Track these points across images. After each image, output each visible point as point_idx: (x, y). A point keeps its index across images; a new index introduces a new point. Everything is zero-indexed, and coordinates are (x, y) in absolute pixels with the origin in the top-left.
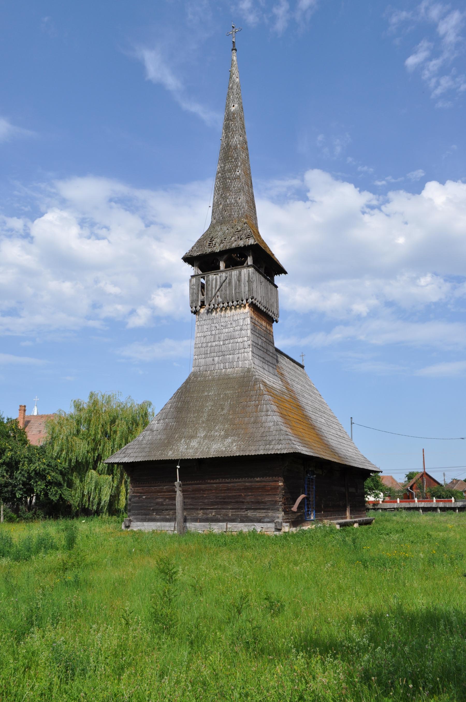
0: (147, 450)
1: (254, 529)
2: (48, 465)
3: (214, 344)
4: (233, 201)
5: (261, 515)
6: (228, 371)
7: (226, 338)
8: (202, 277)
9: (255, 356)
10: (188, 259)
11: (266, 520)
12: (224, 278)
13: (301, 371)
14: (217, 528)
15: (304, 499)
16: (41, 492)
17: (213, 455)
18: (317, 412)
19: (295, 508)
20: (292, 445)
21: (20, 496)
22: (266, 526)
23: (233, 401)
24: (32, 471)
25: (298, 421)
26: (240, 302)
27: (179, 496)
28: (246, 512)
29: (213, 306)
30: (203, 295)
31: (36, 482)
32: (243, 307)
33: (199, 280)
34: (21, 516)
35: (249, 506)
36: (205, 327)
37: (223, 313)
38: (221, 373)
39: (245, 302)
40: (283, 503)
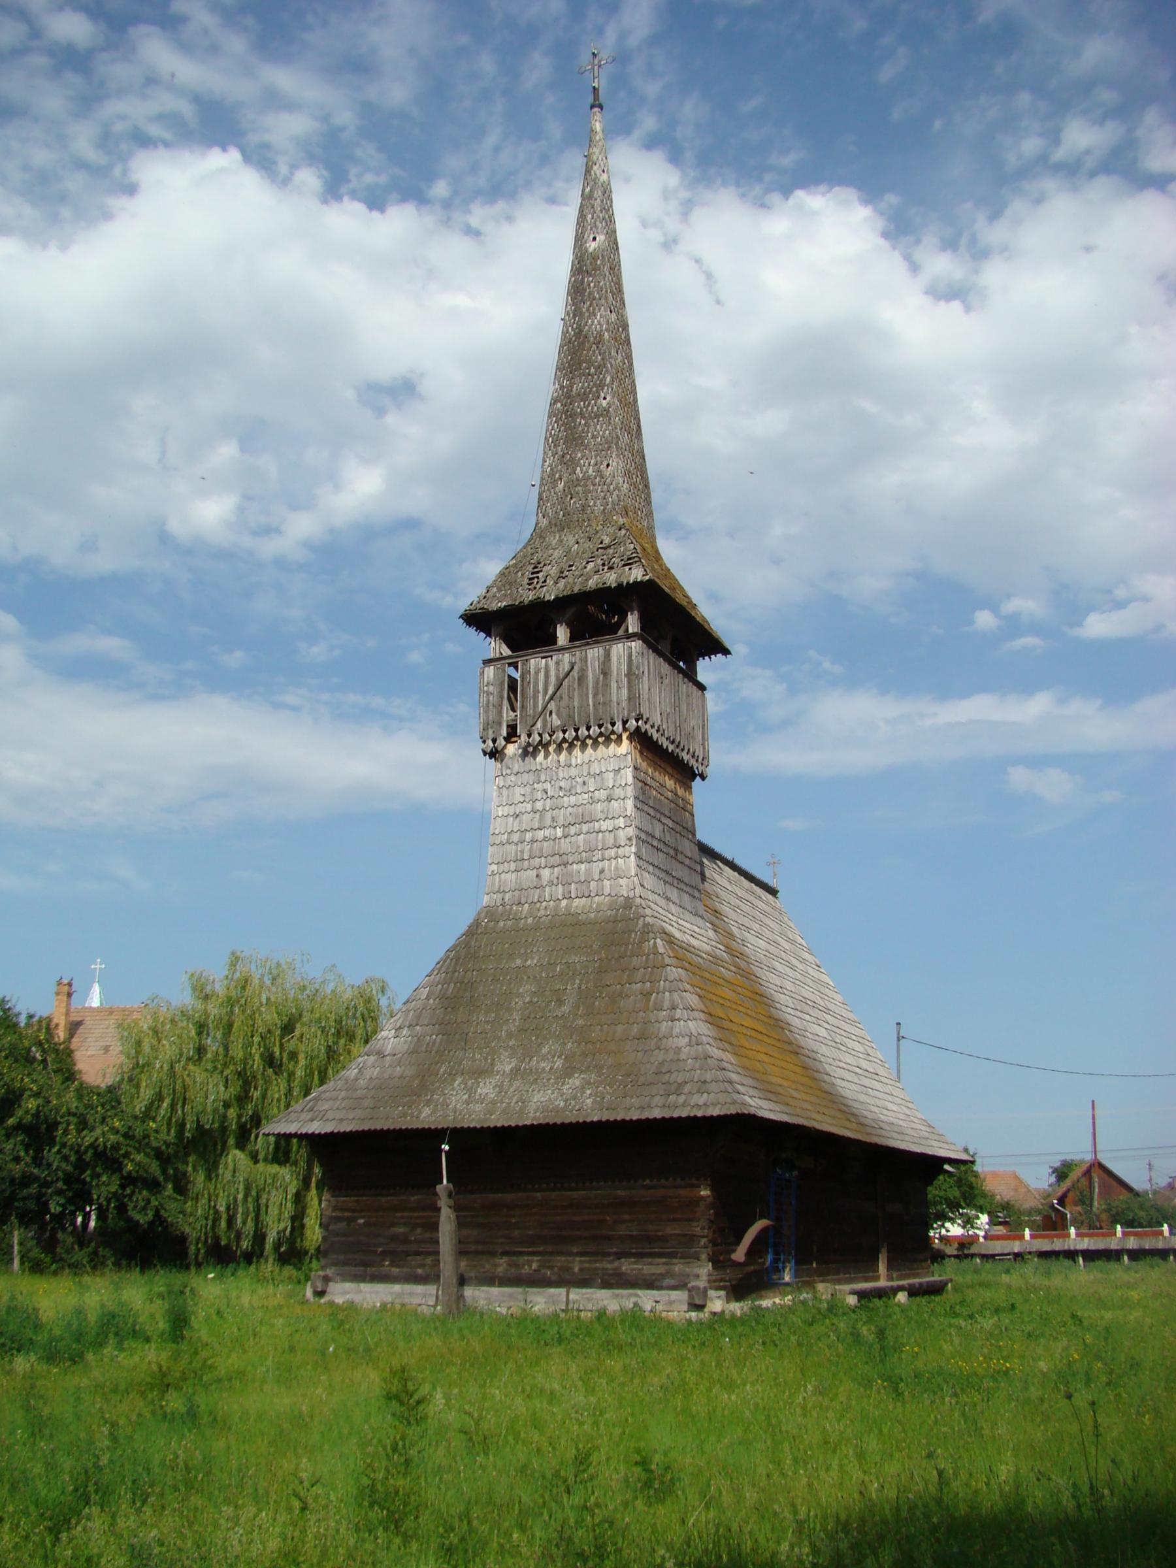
0: (366, 1103)
1: (636, 1304)
2: (126, 1136)
3: (540, 834)
4: (590, 471)
6: (574, 905)
7: (571, 820)
8: (510, 665)
9: (646, 865)
10: (478, 620)
11: (667, 1282)
12: (567, 668)
13: (768, 903)
14: (543, 1302)
15: (764, 1231)
16: (109, 1201)
17: (534, 1118)
18: (807, 1009)
19: (739, 1254)
20: (735, 1096)
21: (59, 1209)
22: (665, 1299)
23: (587, 982)
24: (88, 1148)
25: (754, 1034)
27: (447, 1219)
28: (616, 1264)
29: (538, 739)
30: (514, 710)
31: (98, 1176)
33: (504, 671)
34: (61, 1259)
36: (518, 790)
37: (563, 756)
38: (557, 908)
39: (619, 727)
40: (710, 1241)
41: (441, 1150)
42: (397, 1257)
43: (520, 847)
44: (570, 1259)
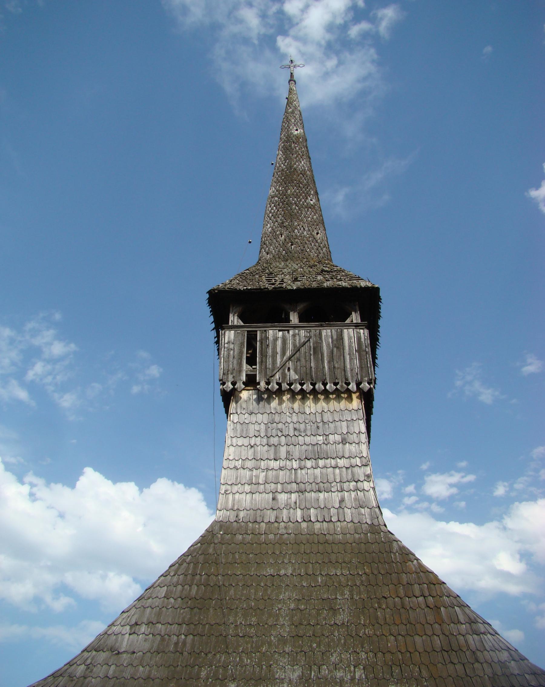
4: (305, 233)
26: (342, 386)
32: (346, 399)
37: (296, 405)
39: (353, 386)
43: (255, 472)
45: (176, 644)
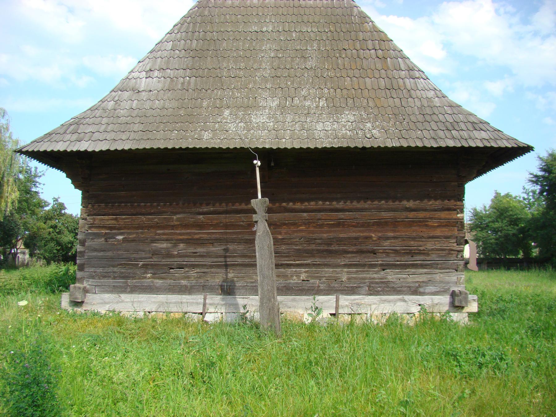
5: (417, 280)
11: (430, 288)
35: (390, 260)
41: (254, 166)
42: (158, 269)
44: (338, 270)
45: (183, 84)
